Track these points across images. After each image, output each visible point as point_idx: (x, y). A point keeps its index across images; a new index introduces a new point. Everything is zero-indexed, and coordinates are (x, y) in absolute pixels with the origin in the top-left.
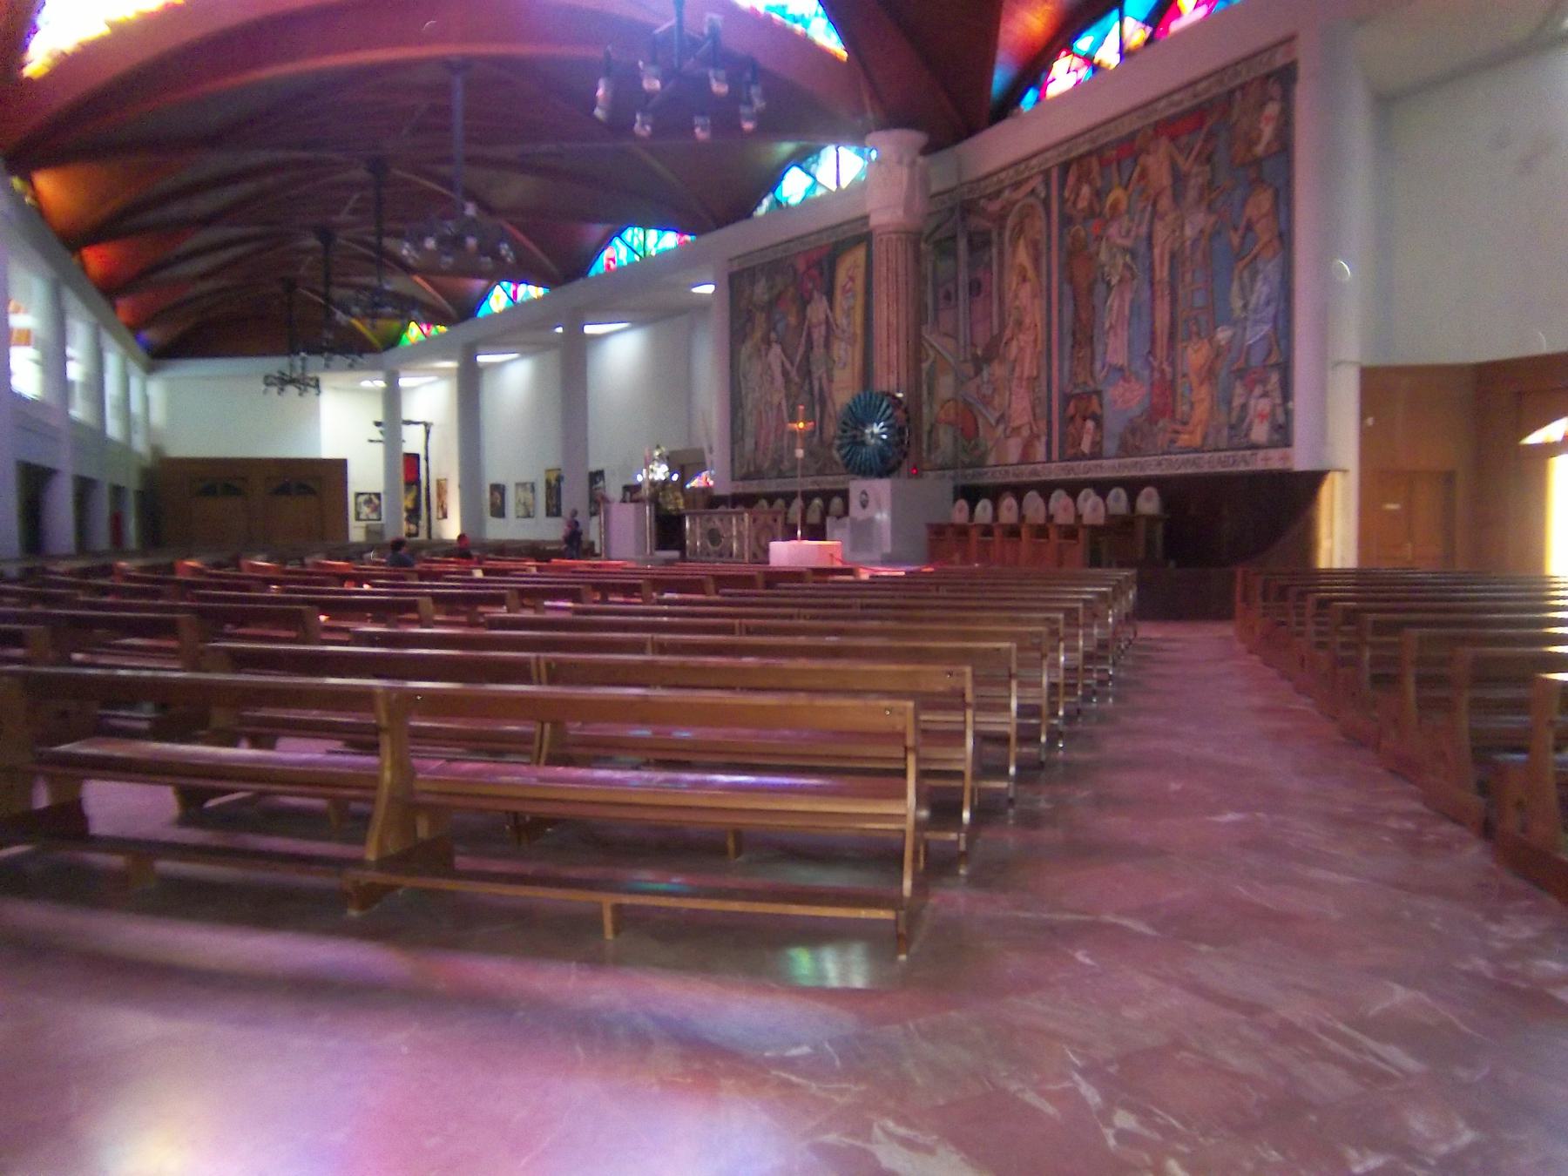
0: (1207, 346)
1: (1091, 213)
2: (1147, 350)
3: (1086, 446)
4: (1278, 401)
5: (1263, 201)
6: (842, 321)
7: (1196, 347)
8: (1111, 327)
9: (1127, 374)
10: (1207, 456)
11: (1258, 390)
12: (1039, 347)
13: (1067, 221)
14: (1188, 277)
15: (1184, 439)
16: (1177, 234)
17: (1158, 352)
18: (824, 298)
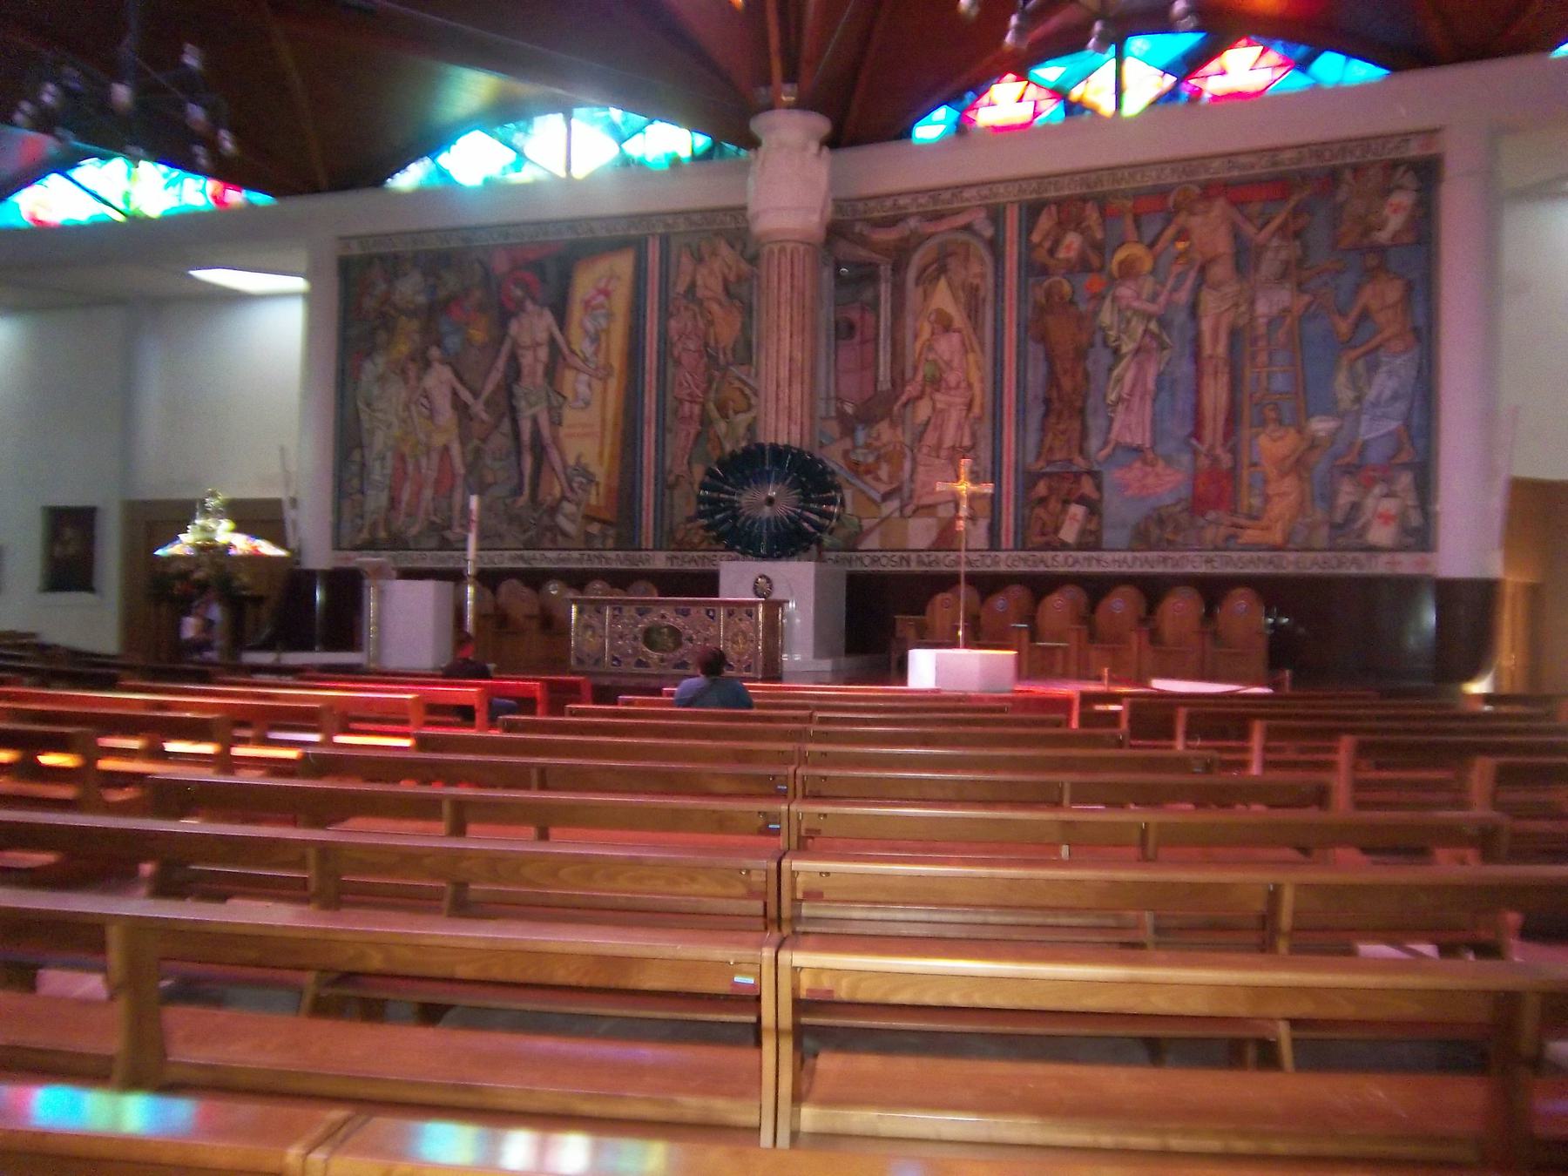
1: (1083, 265)
2: (1189, 429)
3: (1069, 533)
6: (583, 345)
7: (1277, 434)
8: (1120, 399)
9: (1150, 456)
10: (1291, 556)
12: (976, 410)
13: (1033, 269)
14: (1262, 358)
15: (1250, 535)
16: (1243, 309)
17: (1207, 433)
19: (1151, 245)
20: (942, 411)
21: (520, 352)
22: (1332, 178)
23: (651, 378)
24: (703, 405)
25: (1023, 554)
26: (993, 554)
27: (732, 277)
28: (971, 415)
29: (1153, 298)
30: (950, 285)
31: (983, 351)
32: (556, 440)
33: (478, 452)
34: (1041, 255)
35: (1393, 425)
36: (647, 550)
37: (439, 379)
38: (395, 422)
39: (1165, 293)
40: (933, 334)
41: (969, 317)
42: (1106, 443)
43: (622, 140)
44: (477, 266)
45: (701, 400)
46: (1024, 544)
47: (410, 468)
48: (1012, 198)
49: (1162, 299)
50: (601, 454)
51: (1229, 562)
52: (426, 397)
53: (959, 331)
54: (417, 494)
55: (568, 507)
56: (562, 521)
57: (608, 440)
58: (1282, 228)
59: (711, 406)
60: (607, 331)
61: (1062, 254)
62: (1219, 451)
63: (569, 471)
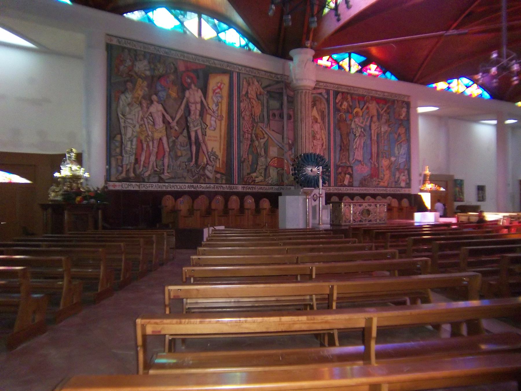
0: (388, 161)
1: (348, 111)
2: (370, 157)
3: (346, 182)
4: (407, 177)
5: (402, 130)
6: (213, 107)
7: (385, 160)
8: (356, 148)
10: (389, 189)
11: (402, 174)
12: (324, 147)
13: (337, 110)
14: (383, 141)
15: (382, 184)
16: (379, 129)
18: (200, 91)
19: (362, 109)
20: (315, 146)
21: (190, 104)
22: (393, 102)
23: (235, 123)
24: (251, 134)
25: (336, 188)
26: (329, 187)
27: (258, 93)
28: (323, 148)
29: (362, 123)
30: (317, 108)
31: (325, 130)
33: (174, 142)
34: (338, 106)
35: (404, 160)
36: (236, 184)
37: (156, 109)
38: (137, 126)
39: (364, 122)
40: (313, 123)
41: (322, 120)
42: (353, 159)
43: (218, 33)
44: (172, 65)
45: (250, 133)
46: (336, 185)
47: (145, 146)
48: (331, 88)
49: (364, 123)
51: (378, 190)
52: (152, 116)
53: (319, 123)
54: (148, 157)
55: (209, 168)
56: (207, 172)
57: (222, 142)
58: (386, 111)
59: (253, 135)
60: (221, 102)
61: (343, 107)
62: (375, 163)
63: (209, 153)
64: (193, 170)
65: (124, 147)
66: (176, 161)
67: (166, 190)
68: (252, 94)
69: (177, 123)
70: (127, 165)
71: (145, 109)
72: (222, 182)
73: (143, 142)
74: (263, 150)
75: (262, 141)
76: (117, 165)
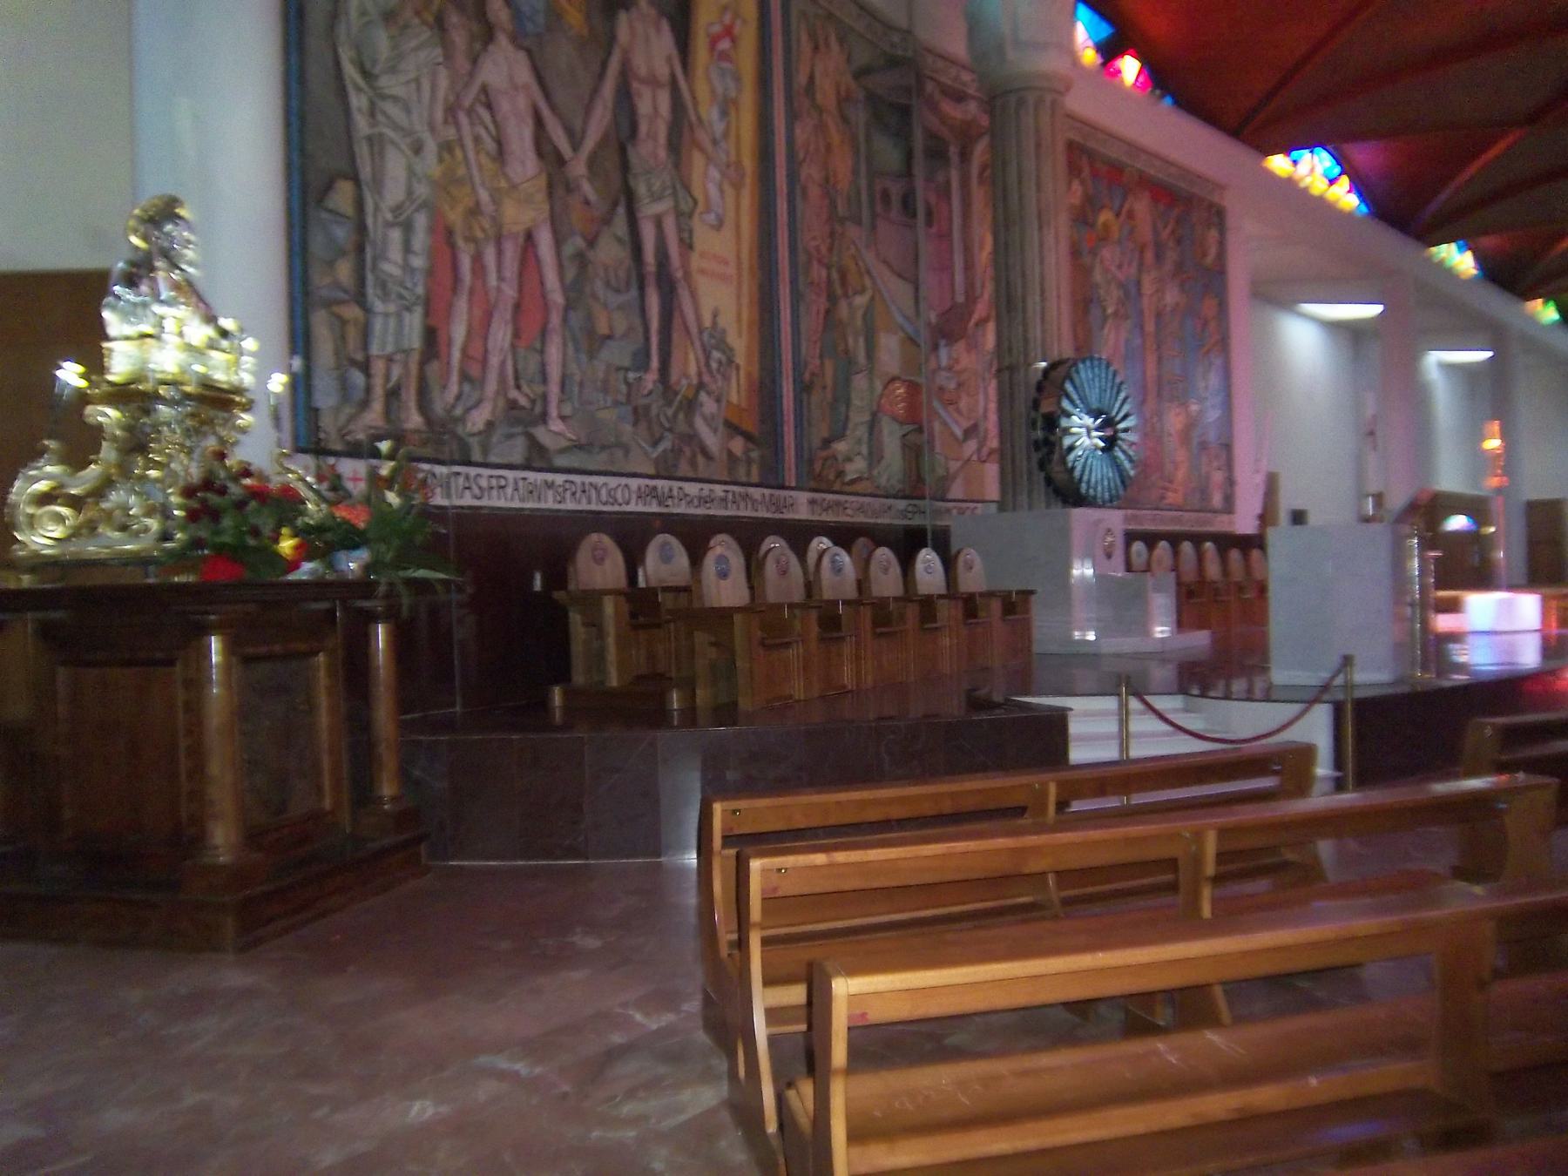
6: (711, 113)
18: (665, 26)
21: (635, 85)
23: (782, 206)
32: (687, 275)
33: (581, 259)
38: (431, 146)
50: (739, 320)
52: (489, 106)
54: (481, 328)
63: (706, 336)
64: (654, 411)
65: (375, 259)
66: (592, 355)
67: (557, 506)
68: (826, 93)
69: (592, 162)
70: (390, 360)
71: (462, 63)
72: (748, 474)
73: (460, 243)
74: (861, 340)
75: (861, 301)
76: (345, 362)
